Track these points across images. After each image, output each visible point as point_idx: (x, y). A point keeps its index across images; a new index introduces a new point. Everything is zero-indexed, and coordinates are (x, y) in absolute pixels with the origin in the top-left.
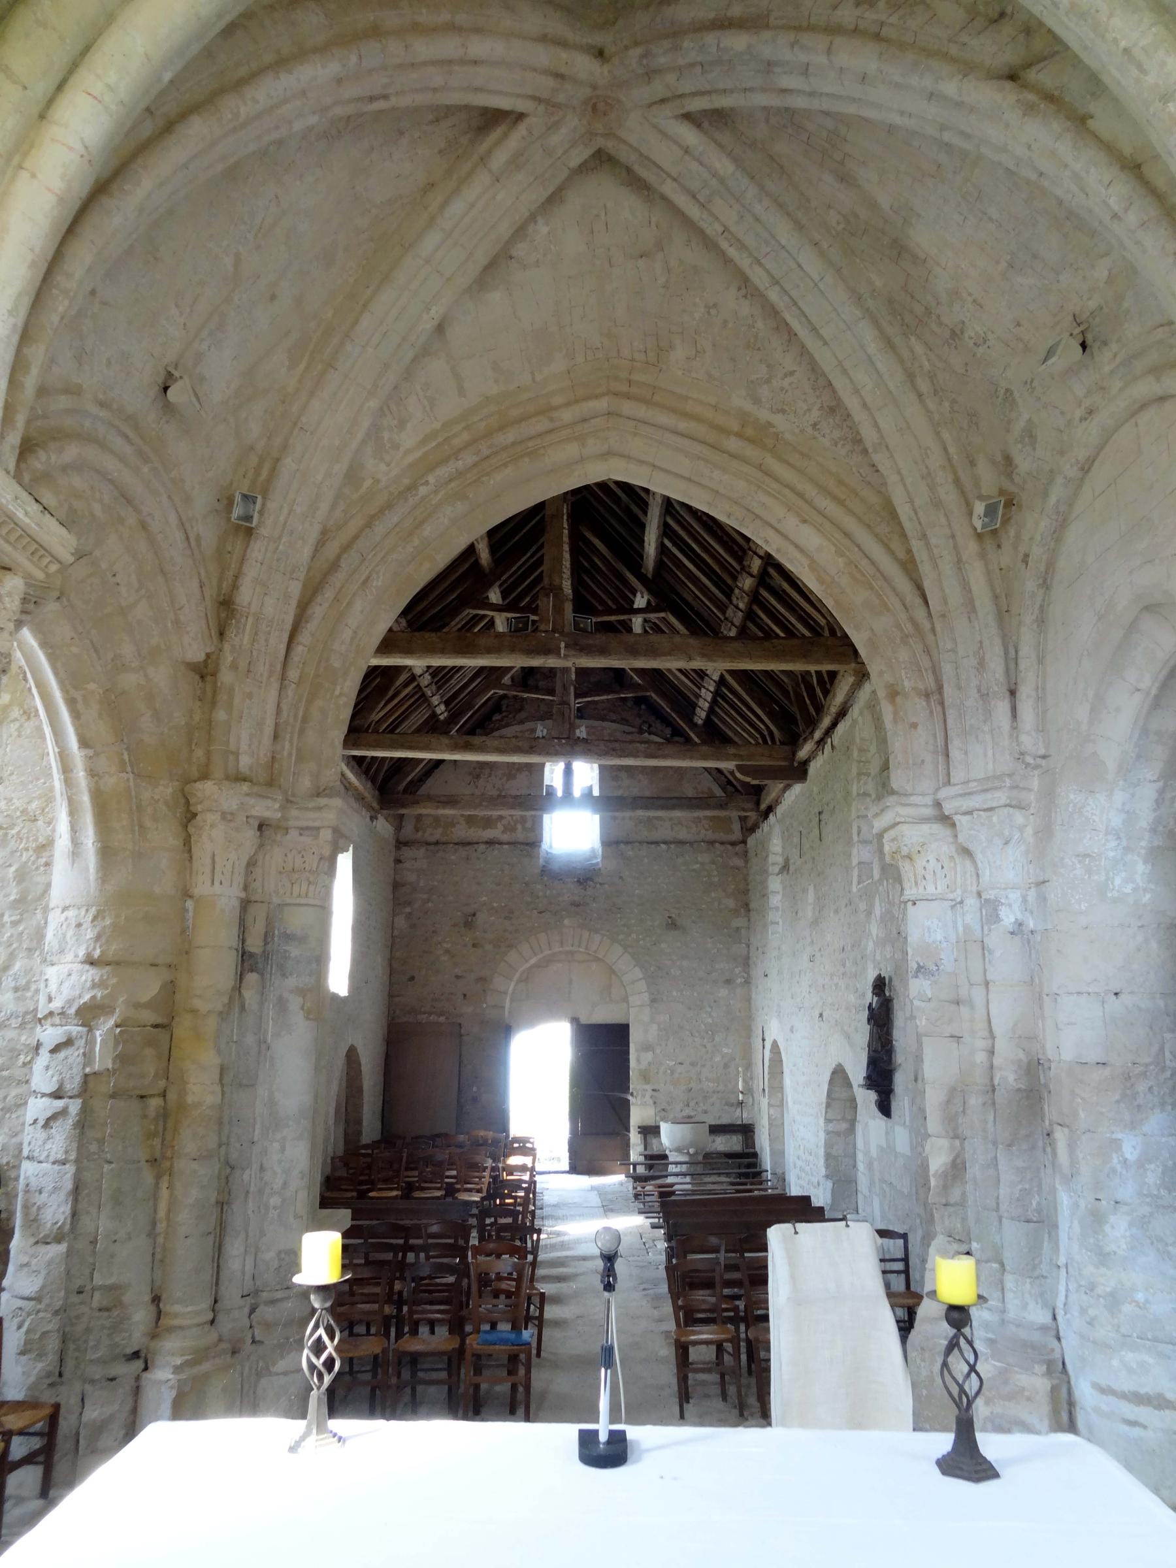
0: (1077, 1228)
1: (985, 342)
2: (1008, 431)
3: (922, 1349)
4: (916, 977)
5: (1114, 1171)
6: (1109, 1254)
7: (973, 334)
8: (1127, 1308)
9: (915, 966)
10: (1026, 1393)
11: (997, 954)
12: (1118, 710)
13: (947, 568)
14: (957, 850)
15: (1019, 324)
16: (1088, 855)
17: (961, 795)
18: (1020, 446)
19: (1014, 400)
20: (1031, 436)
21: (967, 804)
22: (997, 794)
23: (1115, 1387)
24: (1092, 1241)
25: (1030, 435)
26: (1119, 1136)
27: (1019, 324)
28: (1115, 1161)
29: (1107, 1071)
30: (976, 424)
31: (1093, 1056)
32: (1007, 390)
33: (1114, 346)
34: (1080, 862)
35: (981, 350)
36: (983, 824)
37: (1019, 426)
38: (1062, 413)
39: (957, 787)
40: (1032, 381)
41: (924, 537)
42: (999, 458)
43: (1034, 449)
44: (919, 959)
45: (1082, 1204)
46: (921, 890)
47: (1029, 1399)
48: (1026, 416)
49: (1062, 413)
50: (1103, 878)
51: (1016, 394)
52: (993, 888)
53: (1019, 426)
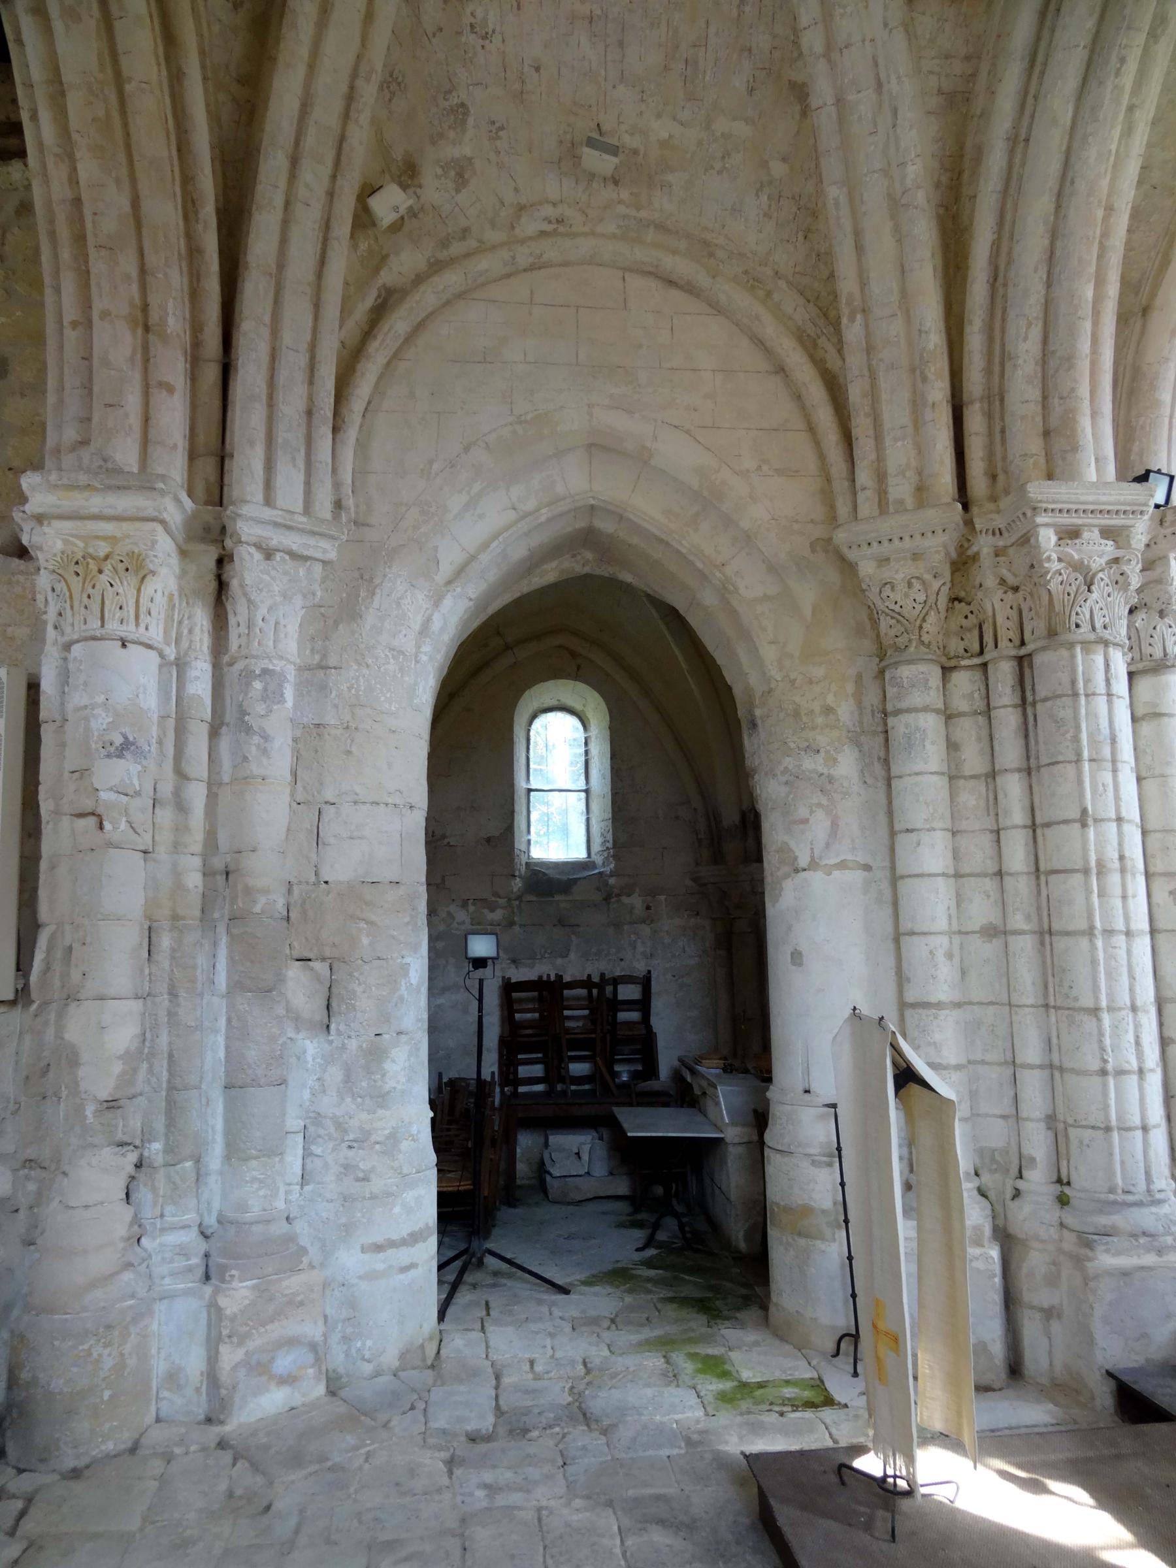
0: (335, 1075)
1: (485, 37)
2: (433, 143)
3: (109, 1327)
4: (120, 756)
5: (401, 998)
6: (389, 1092)
7: (480, 13)
8: (405, 1145)
9: (118, 740)
10: (299, 1298)
11: (277, 743)
12: (482, 516)
13: (308, 221)
14: (181, 590)
15: (537, 69)
16: (402, 653)
17: (276, 525)
18: (439, 171)
19: (464, 122)
20: (460, 175)
21: (278, 538)
22: (324, 544)
23: (395, 1237)
24: (364, 1084)
25: (461, 173)
26: (407, 960)
27: (537, 69)
28: (403, 988)
29: (401, 891)
30: (393, 94)
31: (389, 873)
32: (463, 105)
33: (625, 195)
34: (394, 657)
35: (472, 37)
36: (286, 573)
37: (450, 151)
38: (516, 190)
39: (276, 512)
40: (502, 128)
41: (294, 161)
42: (398, 153)
43: (458, 191)
44: (126, 730)
45: (353, 1044)
46: (142, 629)
47: (302, 1304)
48: (467, 151)
49: (516, 190)
50: (412, 682)
51: (471, 121)
52: (282, 658)
53: (450, 151)
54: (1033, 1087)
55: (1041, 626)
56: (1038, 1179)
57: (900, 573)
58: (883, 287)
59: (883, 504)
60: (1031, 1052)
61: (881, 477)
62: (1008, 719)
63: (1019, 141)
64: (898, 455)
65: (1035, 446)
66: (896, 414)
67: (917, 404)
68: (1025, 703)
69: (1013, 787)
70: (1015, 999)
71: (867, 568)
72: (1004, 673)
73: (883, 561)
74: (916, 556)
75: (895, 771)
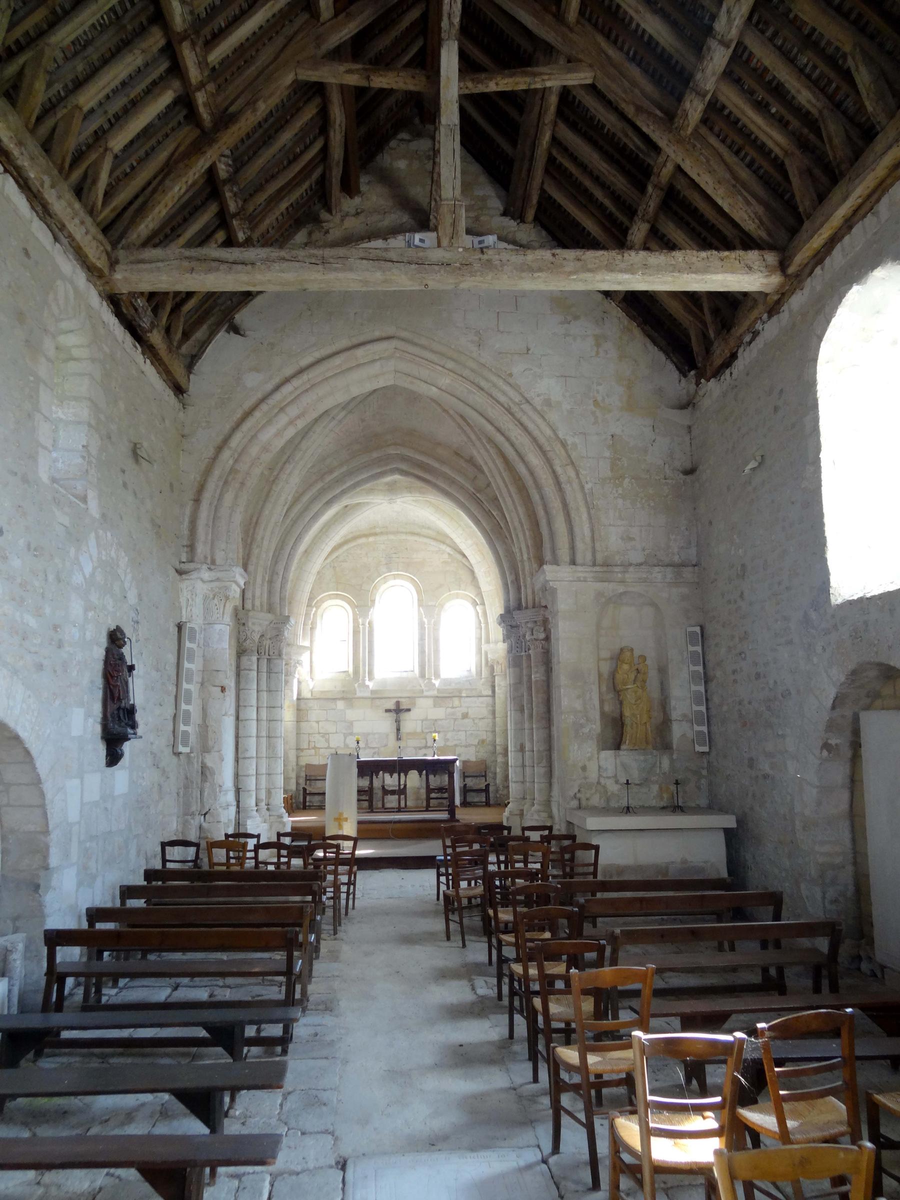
54: (263, 779)
55: (276, 653)
56: (263, 804)
57: (257, 628)
58: (266, 543)
59: (253, 605)
60: (263, 770)
61: (254, 596)
62: (264, 676)
63: (295, 522)
64: (258, 593)
65: (278, 601)
66: (259, 580)
67: (264, 577)
68: (269, 672)
69: (264, 695)
70: (259, 755)
71: (250, 624)
72: (264, 663)
73: (253, 624)
74: (260, 625)
75: (241, 687)
